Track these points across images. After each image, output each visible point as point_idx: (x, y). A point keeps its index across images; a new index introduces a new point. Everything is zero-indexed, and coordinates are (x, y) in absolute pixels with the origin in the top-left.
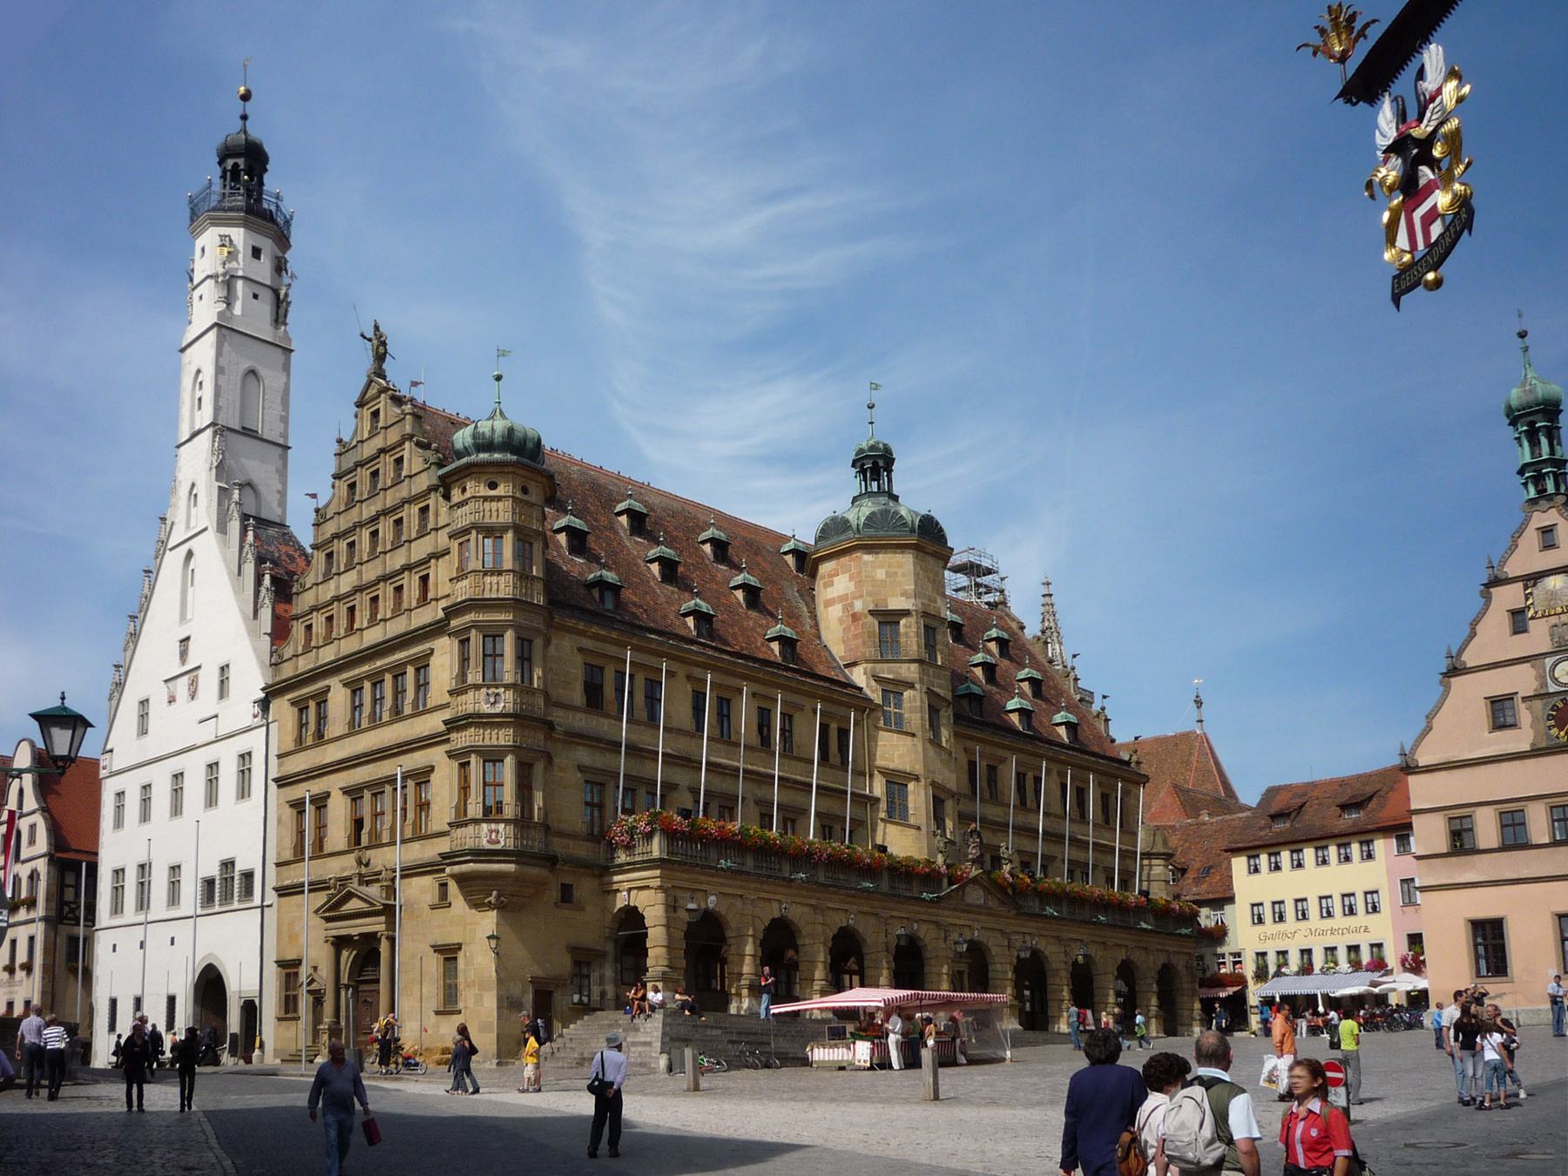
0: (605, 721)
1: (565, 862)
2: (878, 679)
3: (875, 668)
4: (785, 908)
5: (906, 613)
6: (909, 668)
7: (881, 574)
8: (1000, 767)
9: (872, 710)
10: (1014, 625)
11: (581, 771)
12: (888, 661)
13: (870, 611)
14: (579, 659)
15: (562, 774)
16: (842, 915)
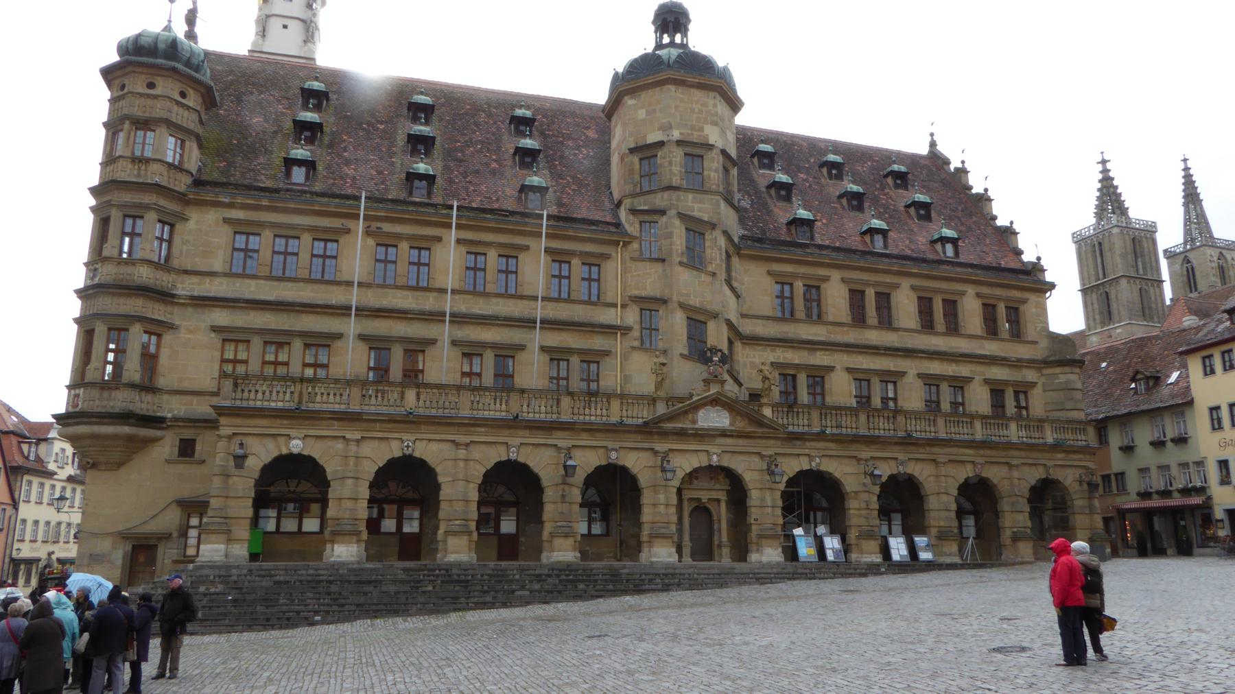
0: (253, 283)
1: (176, 419)
2: (633, 211)
3: (632, 203)
4: (408, 447)
5: (661, 144)
6: (662, 198)
7: (641, 114)
8: (823, 286)
9: (626, 244)
10: (940, 162)
11: (214, 331)
12: (643, 194)
13: (629, 149)
14: (227, 230)
15: (189, 336)
16: (502, 449)
